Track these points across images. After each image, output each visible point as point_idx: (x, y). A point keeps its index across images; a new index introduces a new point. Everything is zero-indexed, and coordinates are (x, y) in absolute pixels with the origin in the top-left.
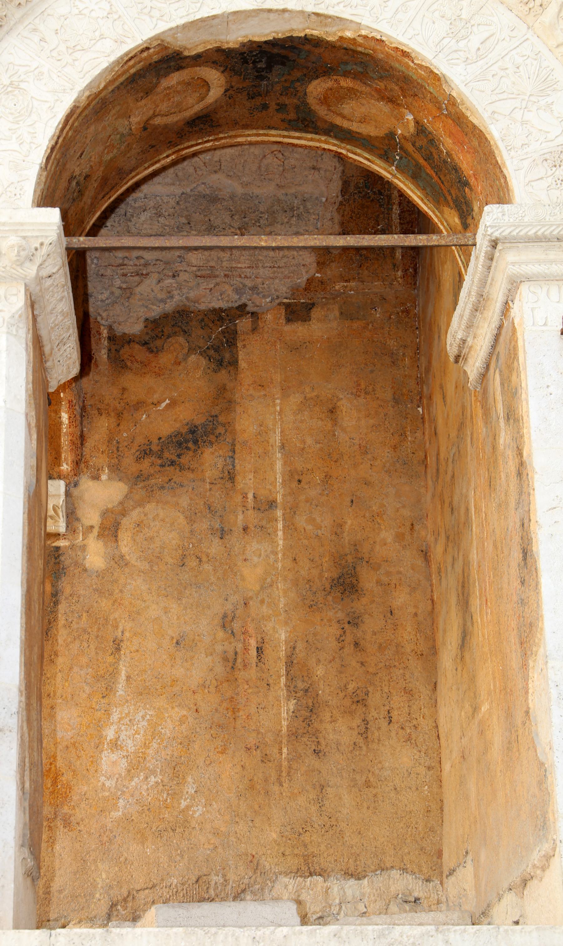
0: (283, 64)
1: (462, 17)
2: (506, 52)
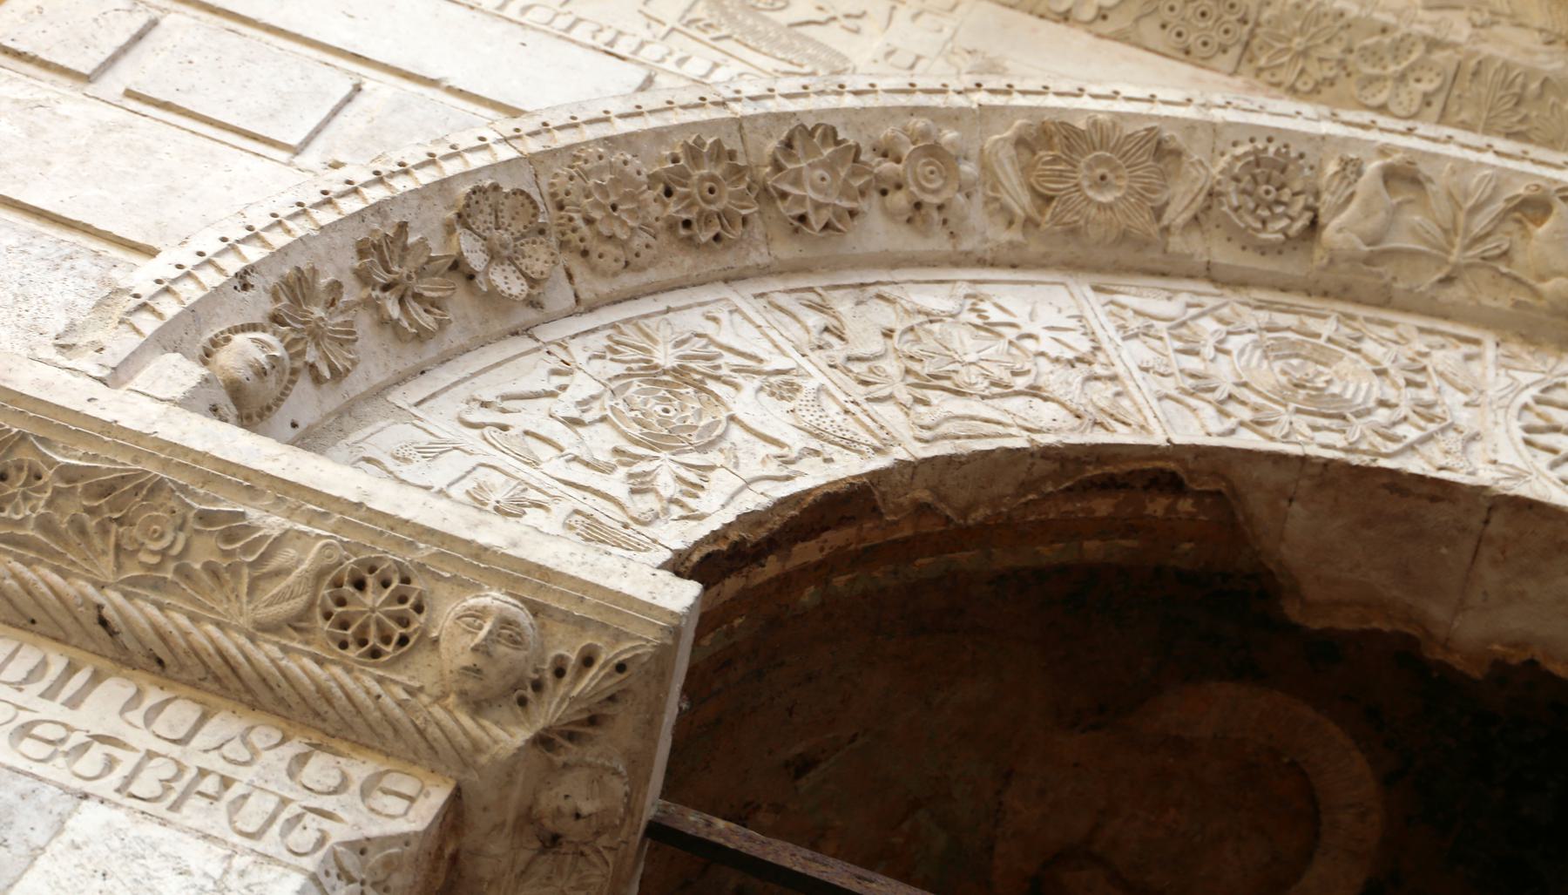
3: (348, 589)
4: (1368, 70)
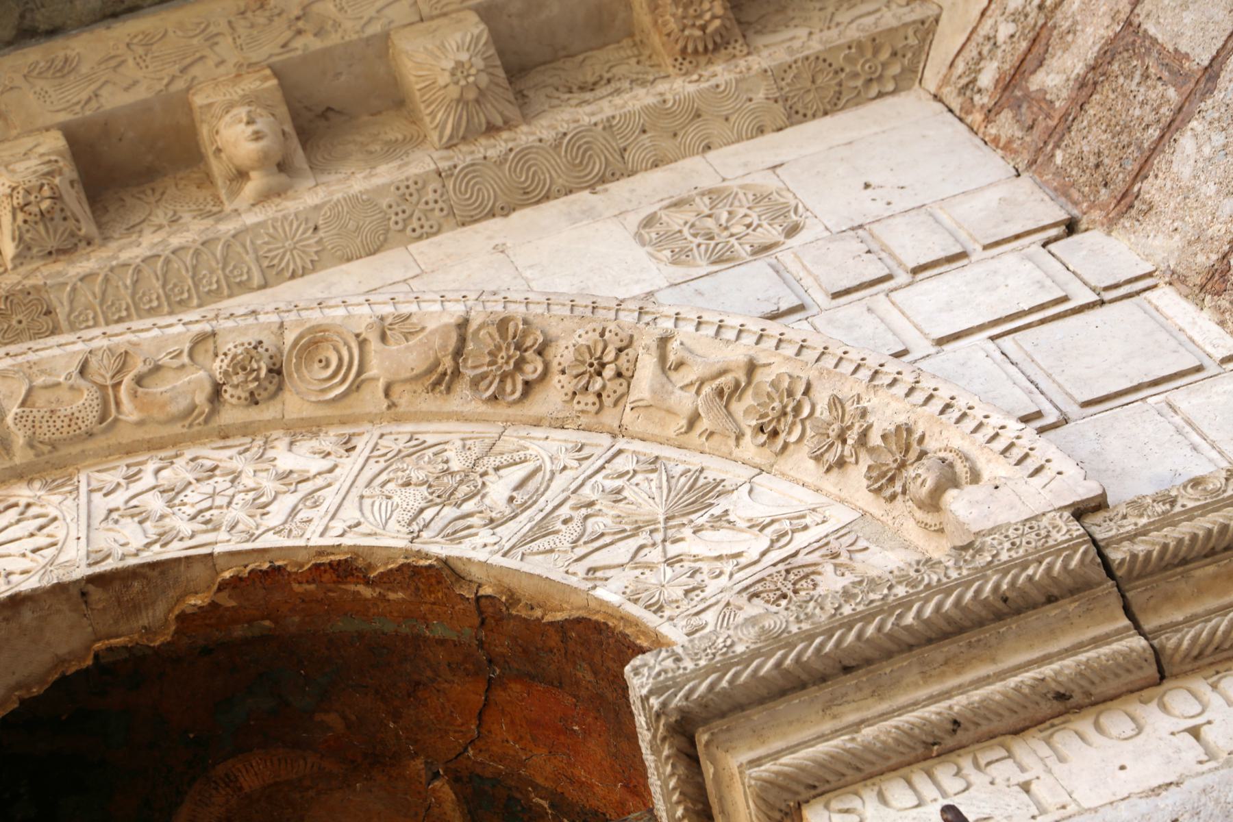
1: (455, 466)
2: (579, 481)
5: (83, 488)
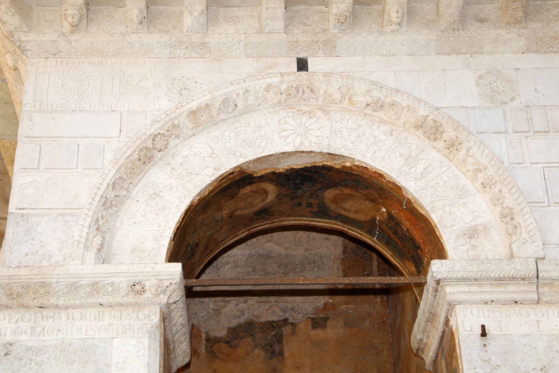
0: (310, 181)
1: (413, 155)
3: (133, 287)
4: (231, 50)
5: (331, 118)
